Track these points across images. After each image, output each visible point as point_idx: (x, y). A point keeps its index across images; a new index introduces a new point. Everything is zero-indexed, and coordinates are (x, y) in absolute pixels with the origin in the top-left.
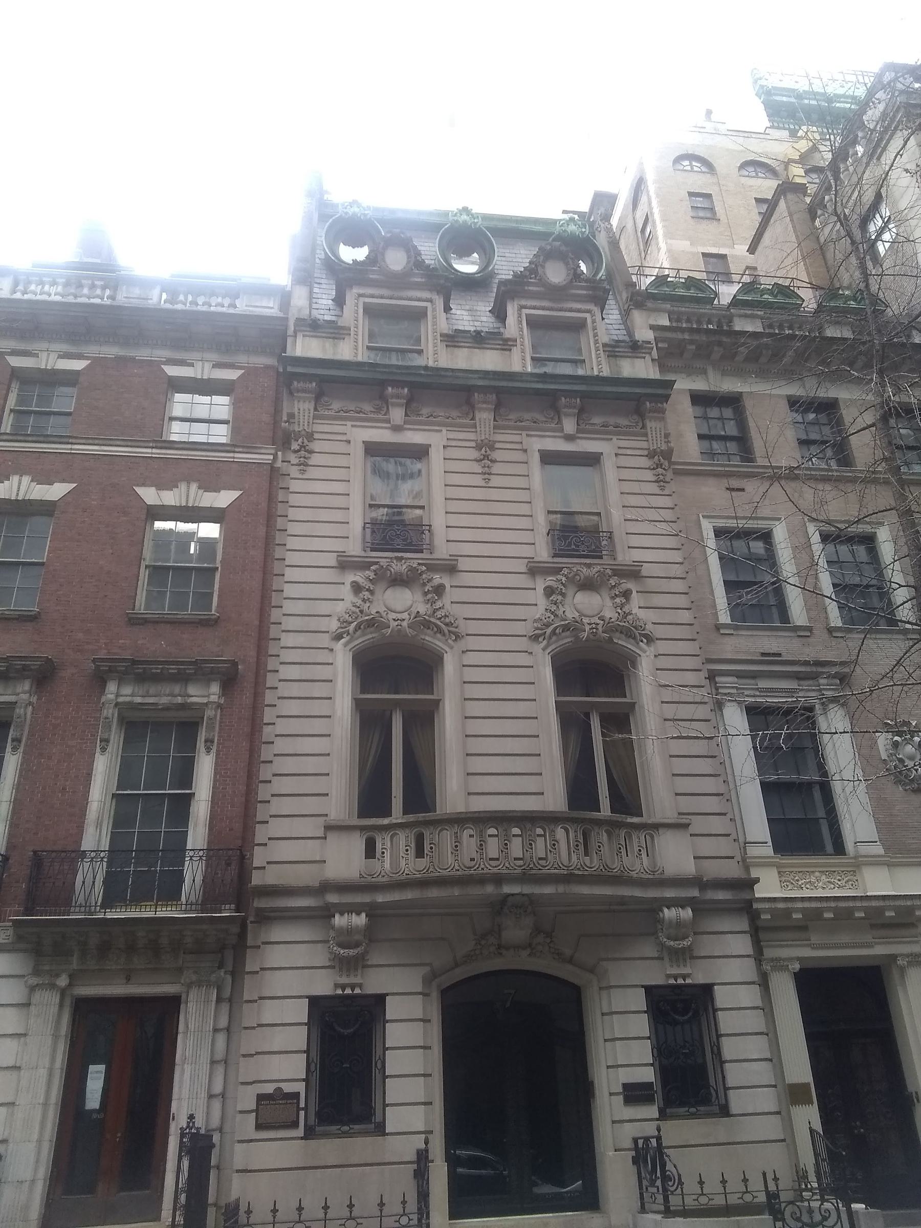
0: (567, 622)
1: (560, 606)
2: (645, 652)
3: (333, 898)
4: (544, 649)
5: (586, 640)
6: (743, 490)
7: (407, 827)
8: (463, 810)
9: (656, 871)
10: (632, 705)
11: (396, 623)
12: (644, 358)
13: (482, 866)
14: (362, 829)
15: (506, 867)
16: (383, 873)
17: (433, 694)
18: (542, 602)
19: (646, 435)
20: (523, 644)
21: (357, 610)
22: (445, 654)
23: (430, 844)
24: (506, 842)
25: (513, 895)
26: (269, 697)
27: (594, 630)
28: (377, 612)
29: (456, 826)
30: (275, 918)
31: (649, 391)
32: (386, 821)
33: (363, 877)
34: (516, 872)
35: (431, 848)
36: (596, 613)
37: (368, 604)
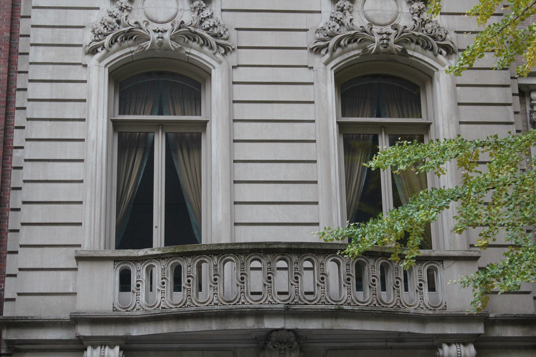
0: (353, 32)
1: (348, 13)
2: (444, 66)
3: (84, 331)
4: (326, 63)
7: (163, 259)
8: (228, 241)
9: (410, 306)
10: (427, 127)
11: (157, 35)
13: (243, 300)
14: (116, 260)
15: (269, 302)
16: (138, 307)
17: (200, 115)
20: (304, 57)
21: (114, 20)
22: (213, 71)
23: (188, 276)
24: (270, 275)
25: (277, 330)
26: (19, 118)
27: (385, 41)
28: (136, 23)
29: (216, 258)
30: (27, 352)
32: (141, 253)
33: (117, 310)
34: (278, 306)
35: (189, 281)
36: (388, 21)
37: (126, 13)
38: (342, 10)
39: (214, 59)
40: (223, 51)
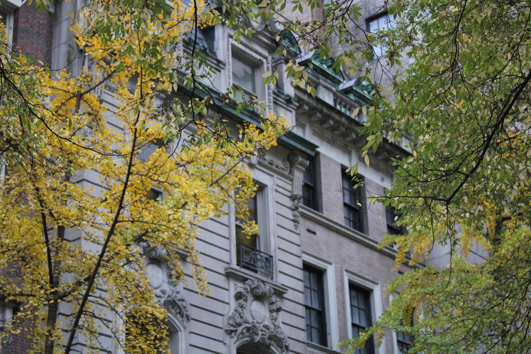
4: (235, 343)
5: (256, 343)
6: (314, 233)
12: (291, 112)
18: (233, 303)
19: (292, 180)
22: (180, 333)
31: (303, 148)
38: (242, 307)
39: (181, 325)
40: (186, 320)
